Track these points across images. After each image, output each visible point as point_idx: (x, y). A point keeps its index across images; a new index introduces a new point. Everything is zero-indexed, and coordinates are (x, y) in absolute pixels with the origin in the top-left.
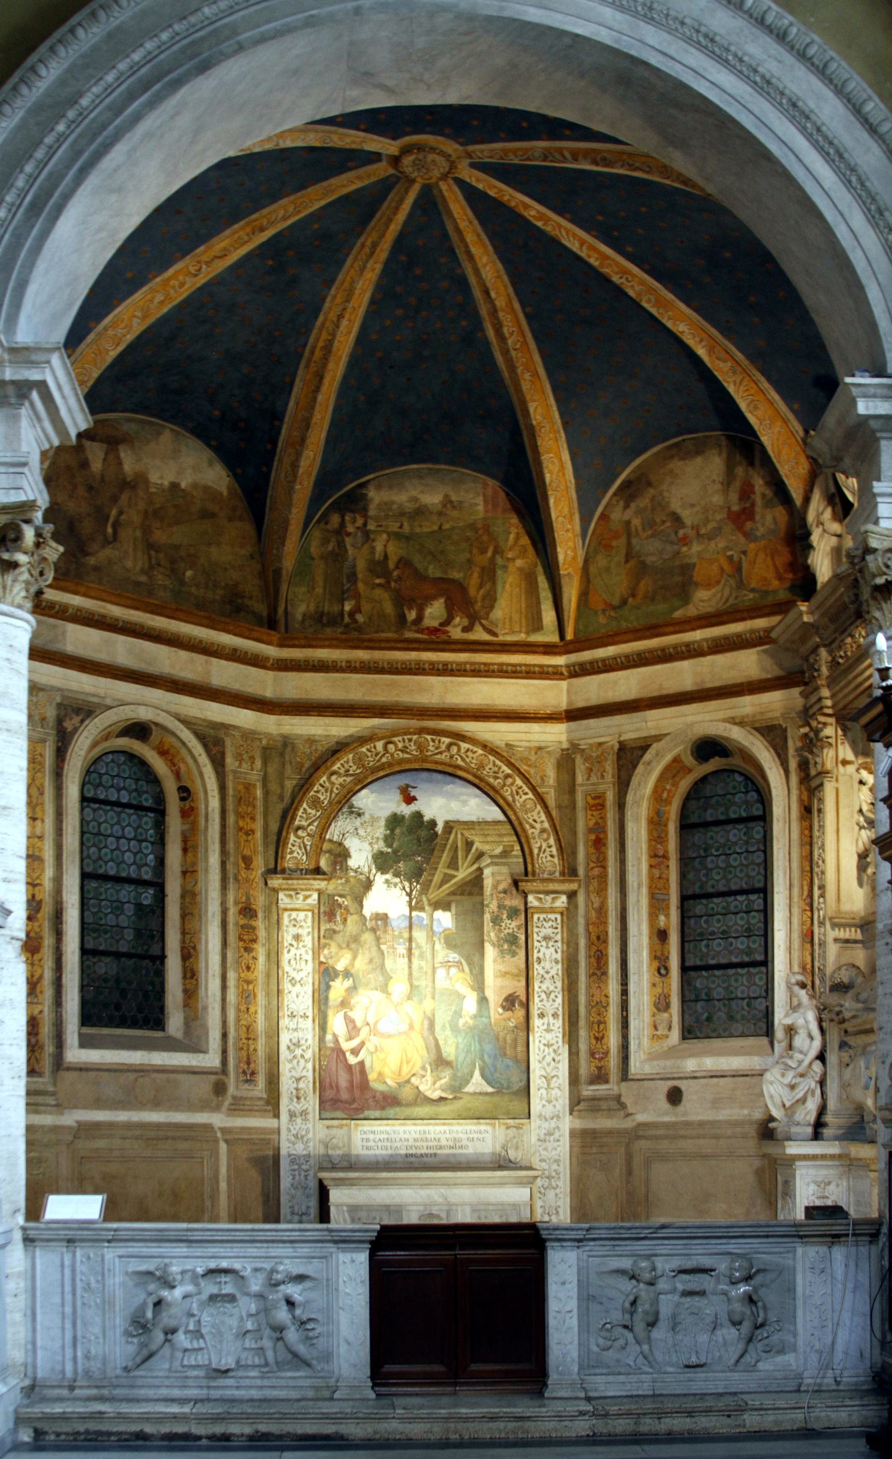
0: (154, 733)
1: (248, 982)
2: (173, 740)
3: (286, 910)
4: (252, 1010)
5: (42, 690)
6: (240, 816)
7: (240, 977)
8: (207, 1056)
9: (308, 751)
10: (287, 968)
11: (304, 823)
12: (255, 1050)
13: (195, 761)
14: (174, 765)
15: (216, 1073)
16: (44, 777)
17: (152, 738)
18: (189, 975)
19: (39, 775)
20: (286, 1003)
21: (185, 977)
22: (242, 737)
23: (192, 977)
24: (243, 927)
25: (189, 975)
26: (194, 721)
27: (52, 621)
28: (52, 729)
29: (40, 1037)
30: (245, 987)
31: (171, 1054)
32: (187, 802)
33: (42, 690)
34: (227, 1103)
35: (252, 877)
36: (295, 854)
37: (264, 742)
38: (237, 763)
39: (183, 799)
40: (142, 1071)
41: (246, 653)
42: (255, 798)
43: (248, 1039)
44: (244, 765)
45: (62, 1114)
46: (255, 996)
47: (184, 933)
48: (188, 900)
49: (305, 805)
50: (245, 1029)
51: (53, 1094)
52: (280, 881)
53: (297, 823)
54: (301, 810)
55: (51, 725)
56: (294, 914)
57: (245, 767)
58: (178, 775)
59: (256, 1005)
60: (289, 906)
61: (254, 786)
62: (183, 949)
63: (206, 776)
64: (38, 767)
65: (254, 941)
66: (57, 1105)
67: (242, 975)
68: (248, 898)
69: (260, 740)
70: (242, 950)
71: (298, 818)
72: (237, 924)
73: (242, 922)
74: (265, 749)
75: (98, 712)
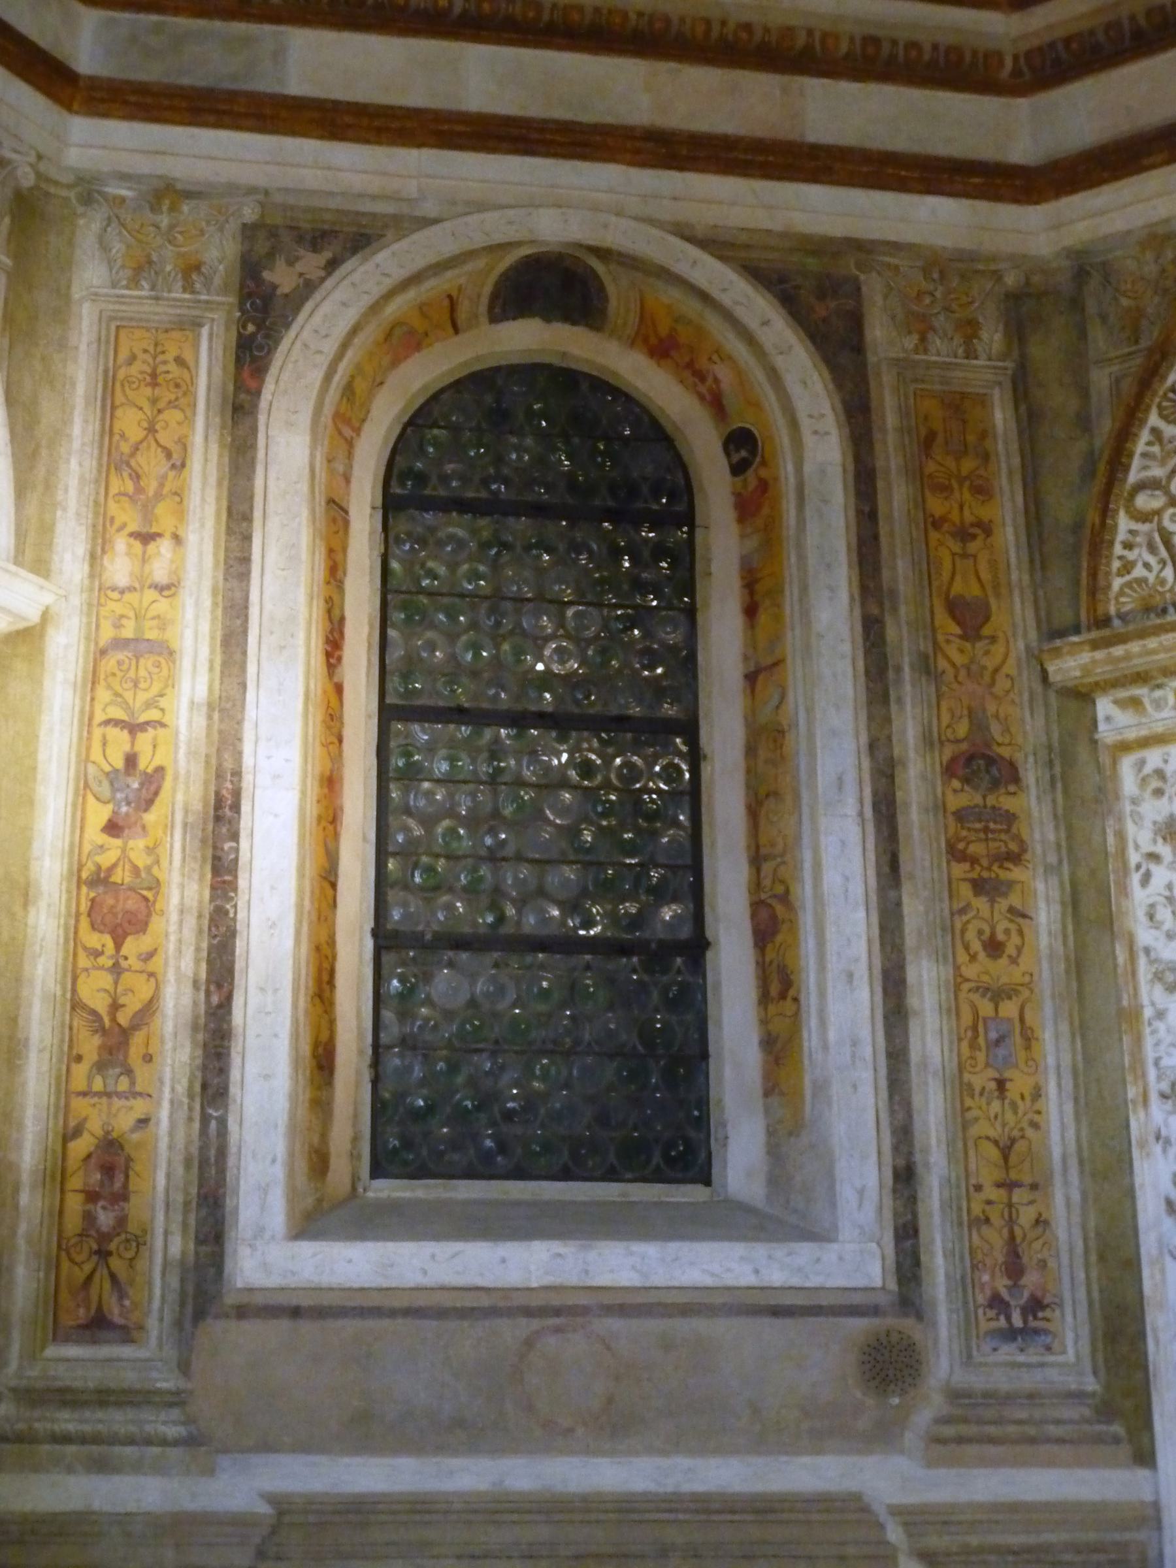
0: (611, 289)
1: (998, 995)
2: (672, 295)
3: (1125, 747)
4: (1019, 1084)
5: (189, 195)
6: (923, 482)
7: (959, 979)
8: (830, 1253)
9: (1151, 269)
10: (1145, 936)
11: (1158, 472)
12: (1041, 1222)
13: (750, 339)
14: (701, 376)
15: (875, 1311)
16: (189, 420)
17: (613, 303)
18: (774, 989)
19: (173, 416)
20: (1150, 1053)
21: (764, 998)
22: (926, 271)
23: (783, 996)
24: (960, 816)
25: (774, 989)
26: (743, 238)
27: (240, 27)
28: (225, 289)
29: (135, 1208)
30: (986, 1008)
31: (673, 1247)
32: (750, 473)
33: (189, 195)
34: (923, 1418)
35: (990, 663)
36: (1139, 572)
37: (1011, 280)
38: (910, 342)
39: (738, 469)
40: (557, 1312)
41: (913, 45)
42: (983, 435)
43: (1009, 1185)
44: (937, 343)
45: (210, 1471)
46: (1029, 1038)
47: (757, 859)
48: (763, 754)
49: (1154, 419)
50: (994, 1153)
51: (176, 1400)
52: (1086, 657)
53: (1133, 477)
54: (1145, 436)
55: (217, 281)
56: (1153, 758)
57: (941, 349)
58: (716, 404)
59: (1034, 1065)
60: (1131, 735)
61: (983, 401)
62: (757, 906)
63: (791, 382)
64: (168, 395)
65: (1015, 858)
66: (191, 1441)
67: (970, 971)
68: (978, 724)
69: (997, 276)
70: (966, 890)
71: (1136, 462)
72: (940, 807)
73: (955, 802)
74: (1015, 298)
75: (390, 234)
